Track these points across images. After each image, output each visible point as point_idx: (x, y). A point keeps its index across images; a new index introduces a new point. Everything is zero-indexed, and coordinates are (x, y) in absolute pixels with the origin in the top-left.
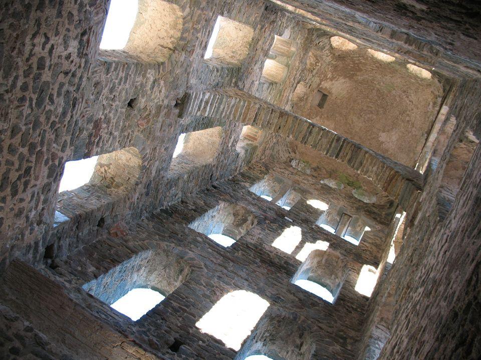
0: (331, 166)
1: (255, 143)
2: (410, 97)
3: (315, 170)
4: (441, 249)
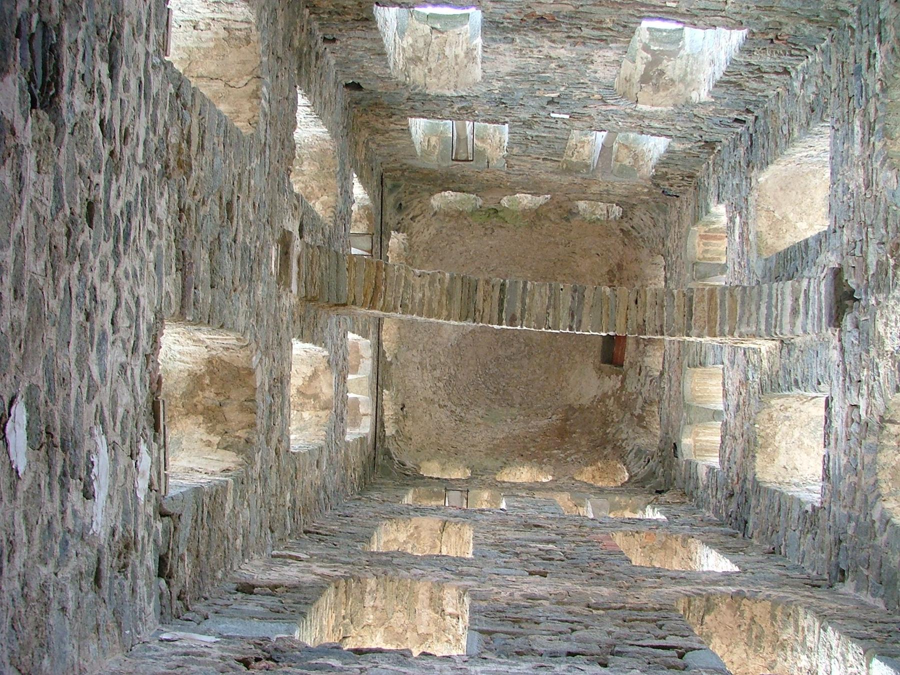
0: (544, 233)
1: (699, 229)
2: (449, 413)
3: (570, 212)
4: (118, 298)
